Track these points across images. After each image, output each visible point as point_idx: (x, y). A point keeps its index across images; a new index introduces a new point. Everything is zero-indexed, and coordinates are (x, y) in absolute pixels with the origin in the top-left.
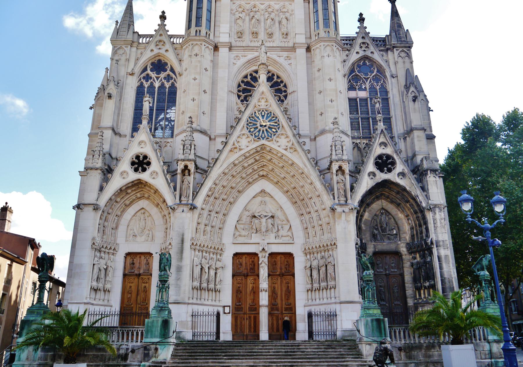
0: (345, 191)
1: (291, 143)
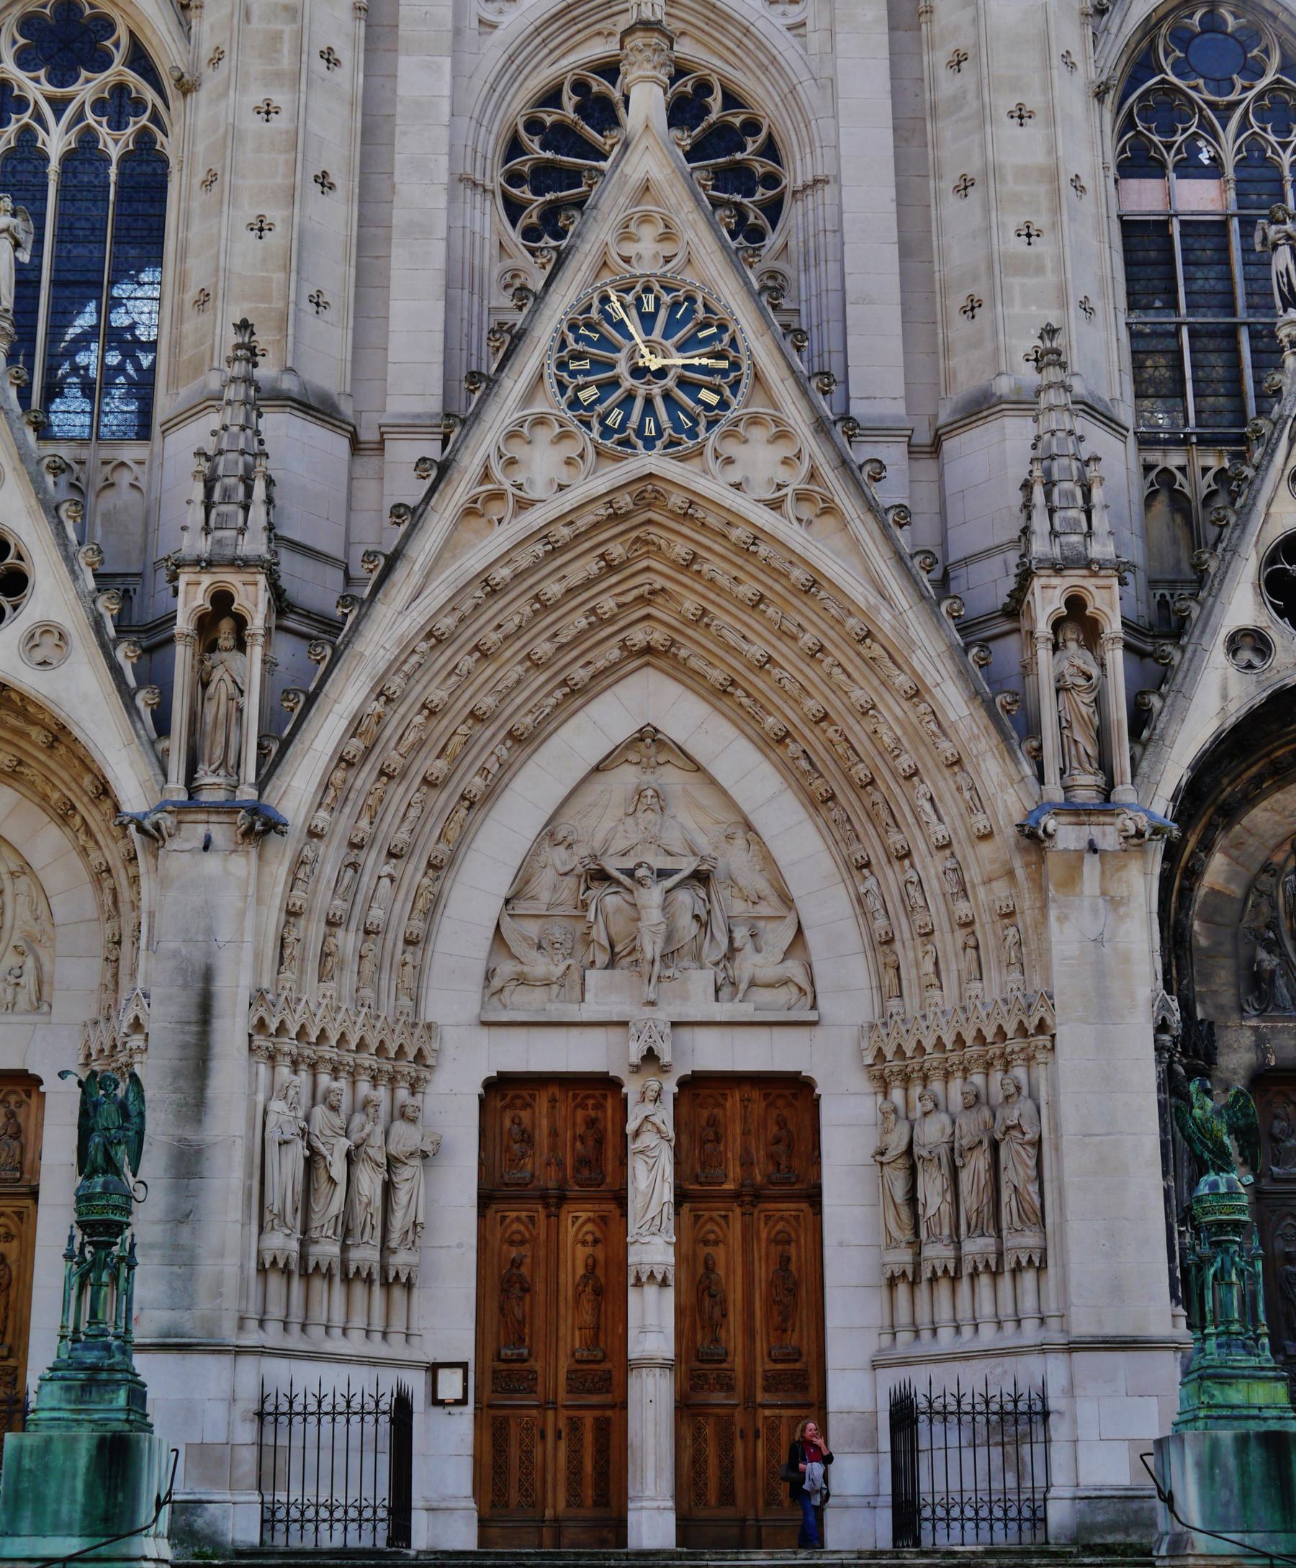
0: (1102, 736)
1: (804, 468)
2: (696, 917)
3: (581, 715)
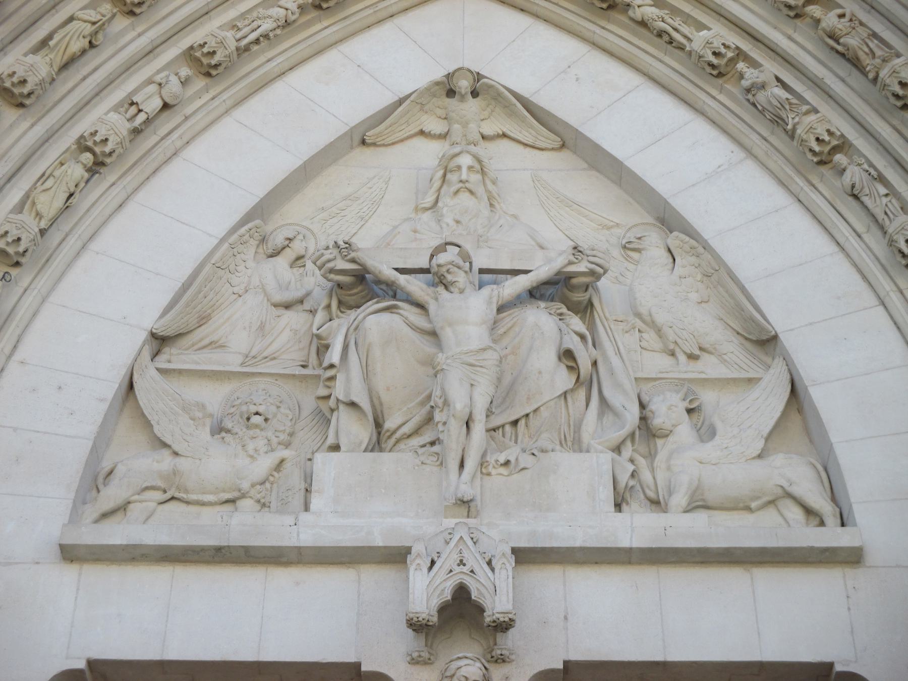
2: (567, 355)
3: (333, 55)
